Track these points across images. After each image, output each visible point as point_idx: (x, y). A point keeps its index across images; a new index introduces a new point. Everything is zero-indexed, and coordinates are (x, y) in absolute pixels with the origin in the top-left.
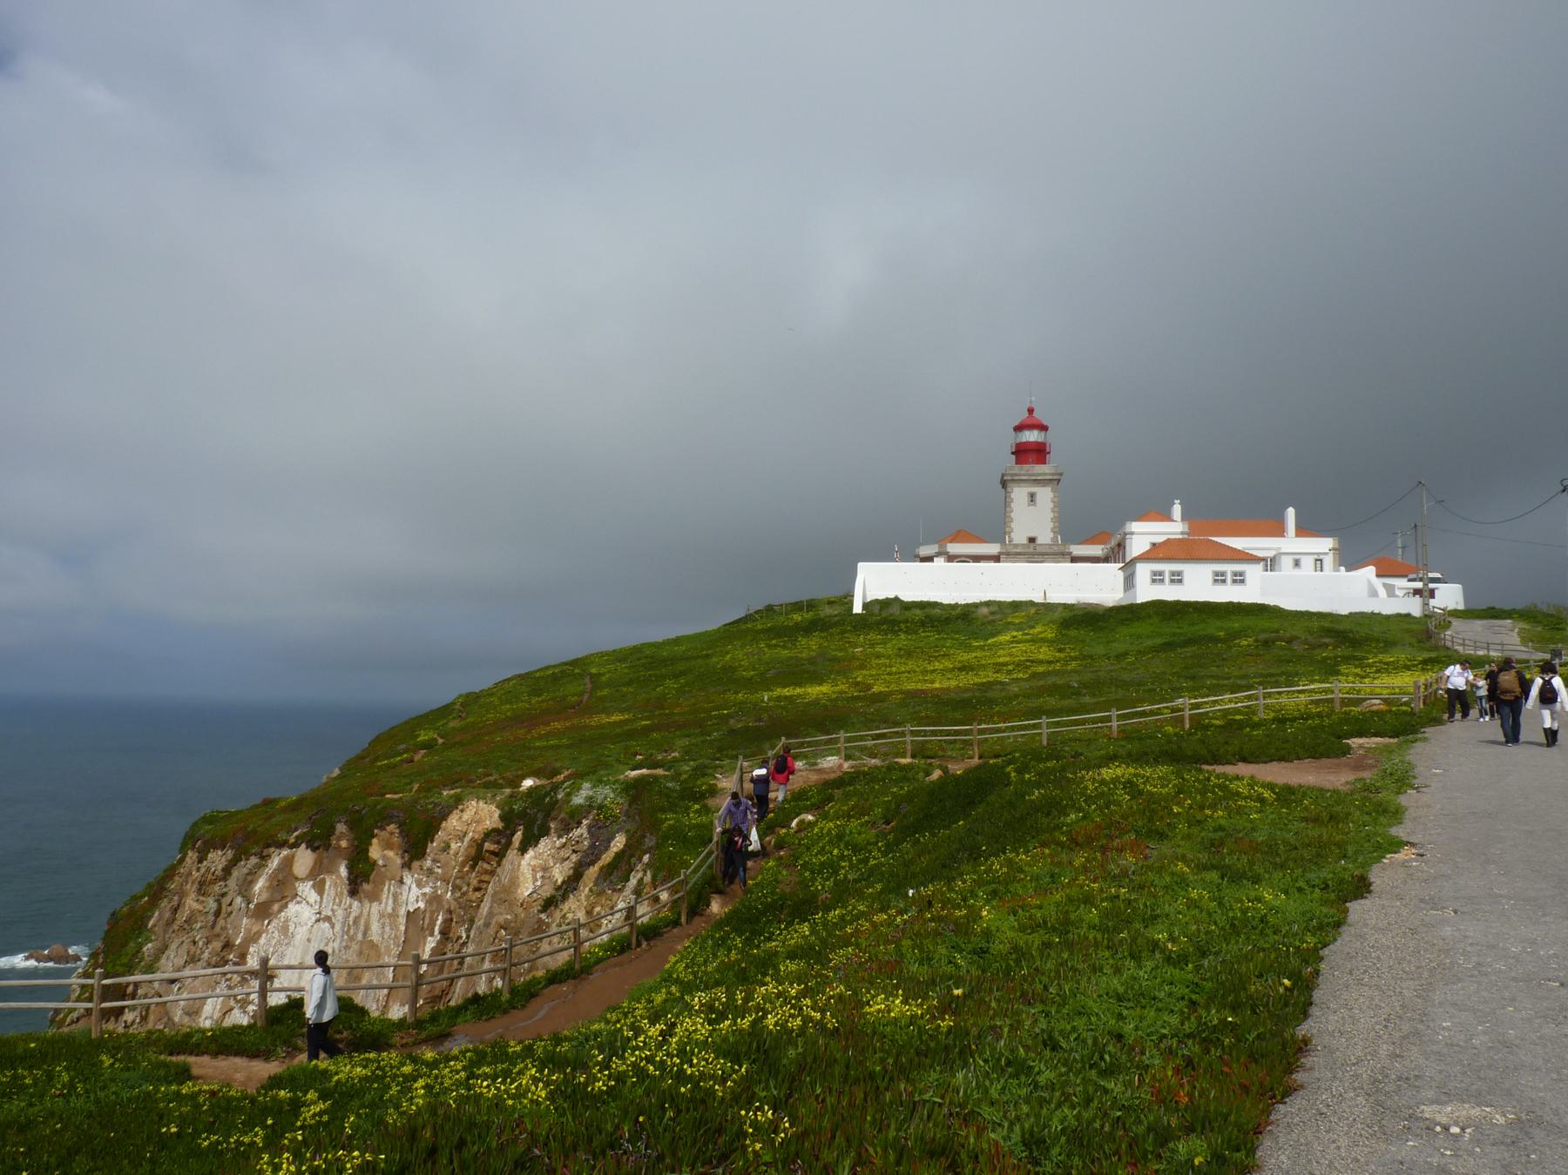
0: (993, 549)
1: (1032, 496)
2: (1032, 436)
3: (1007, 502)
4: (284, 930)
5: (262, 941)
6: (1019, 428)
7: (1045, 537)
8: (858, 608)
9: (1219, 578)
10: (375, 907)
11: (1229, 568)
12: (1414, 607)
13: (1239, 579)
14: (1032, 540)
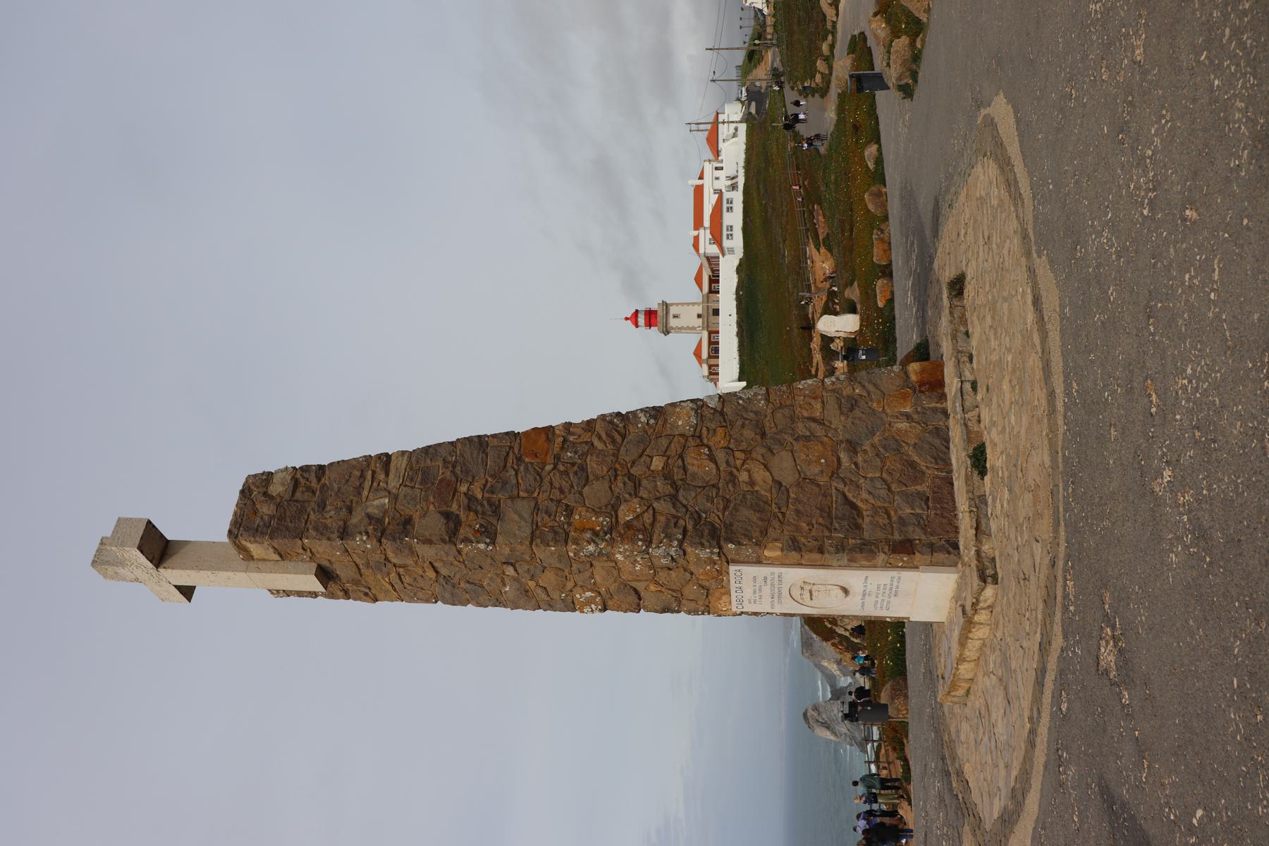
0: (705, 334)
1: (675, 316)
2: (641, 320)
3: (680, 329)
6: (637, 326)
8: (744, 384)
9: (730, 209)
11: (725, 206)
12: (743, 128)
13: (730, 201)
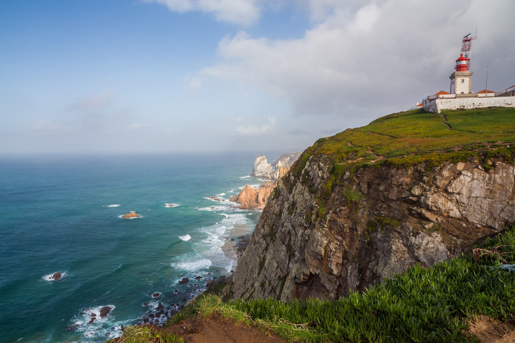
0: (454, 96)
1: (463, 81)
3: (453, 83)
4: (461, 181)
5: (453, 185)
6: (456, 61)
7: (466, 92)
8: (439, 112)
10: (496, 175)
14: (463, 93)
